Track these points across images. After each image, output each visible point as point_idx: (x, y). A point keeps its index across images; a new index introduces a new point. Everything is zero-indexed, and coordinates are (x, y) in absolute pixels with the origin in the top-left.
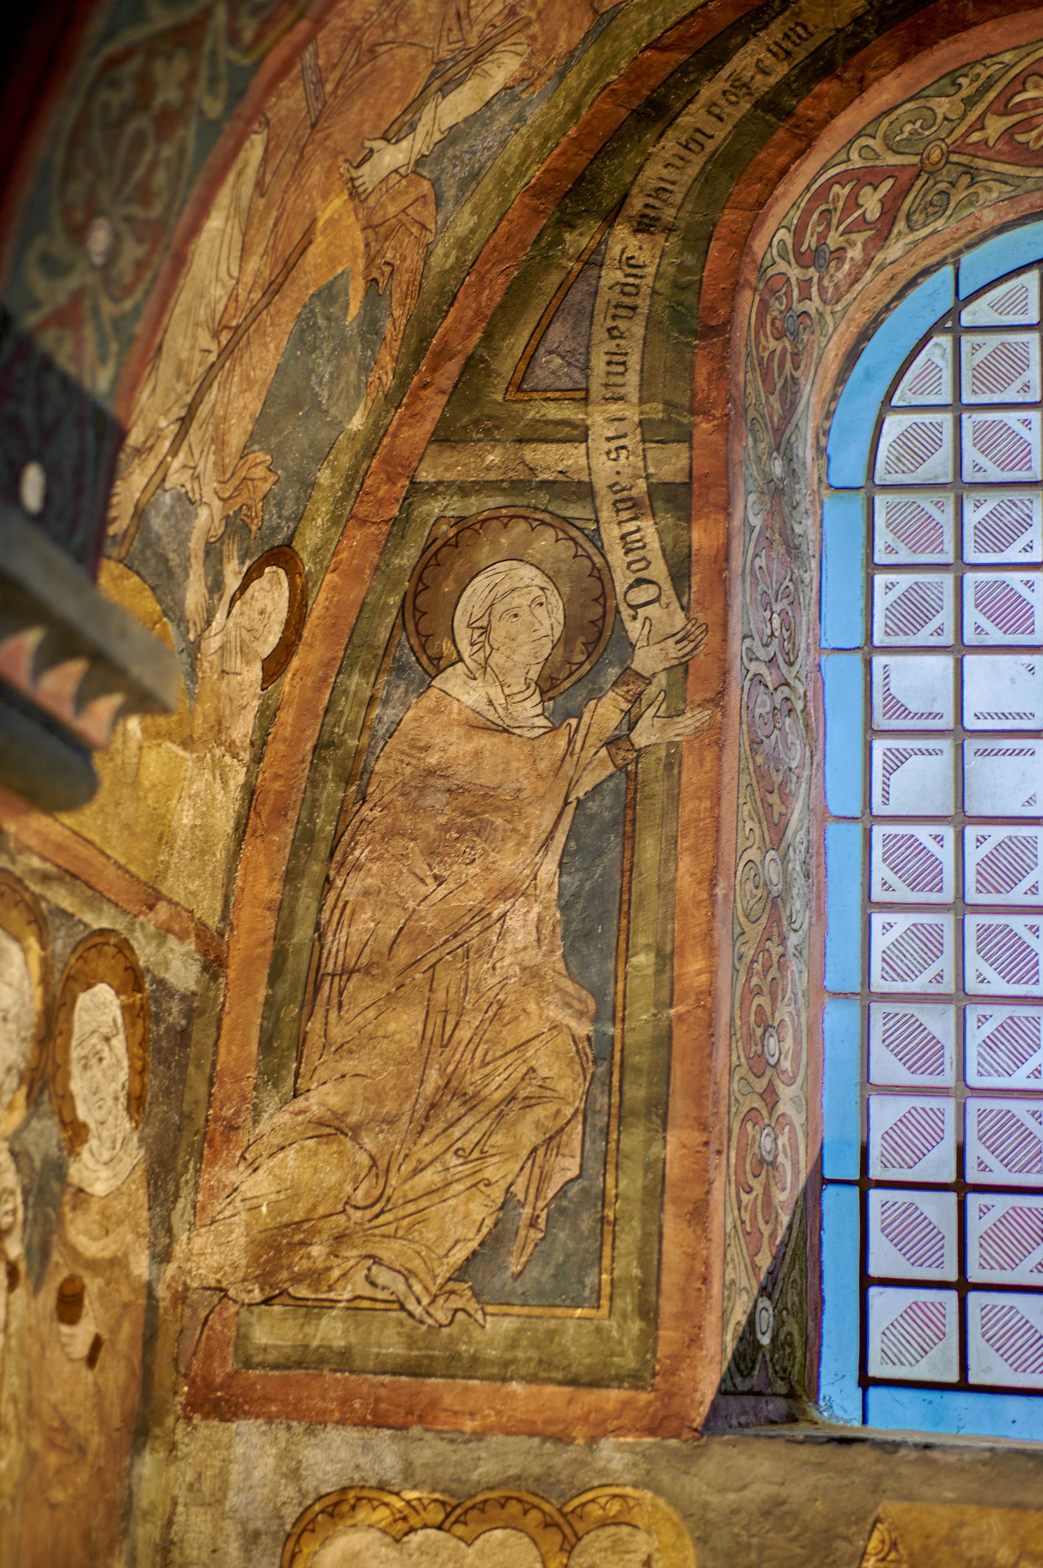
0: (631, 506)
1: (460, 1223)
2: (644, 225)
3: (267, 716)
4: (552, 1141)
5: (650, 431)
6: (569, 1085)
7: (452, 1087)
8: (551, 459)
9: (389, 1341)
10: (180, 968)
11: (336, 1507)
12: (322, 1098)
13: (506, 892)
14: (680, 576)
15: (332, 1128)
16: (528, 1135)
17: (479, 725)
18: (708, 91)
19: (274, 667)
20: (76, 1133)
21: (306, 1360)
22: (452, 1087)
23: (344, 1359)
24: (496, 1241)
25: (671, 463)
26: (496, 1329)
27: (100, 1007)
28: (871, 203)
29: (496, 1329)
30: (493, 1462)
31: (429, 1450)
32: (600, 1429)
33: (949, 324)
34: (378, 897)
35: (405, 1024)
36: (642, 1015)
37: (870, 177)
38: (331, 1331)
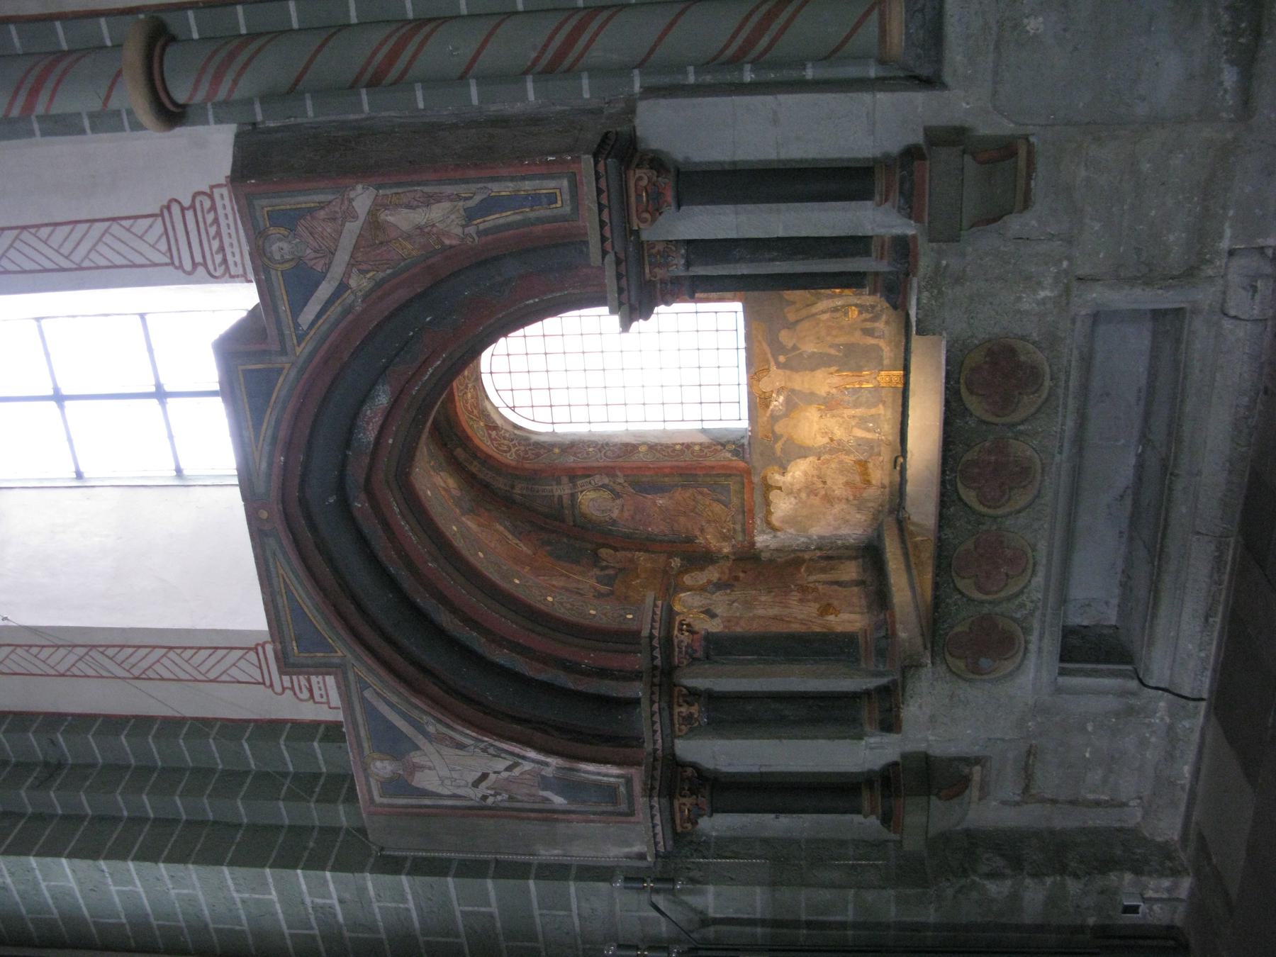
0: (575, 486)
1: (718, 508)
2: (513, 487)
3: (623, 549)
4: (701, 493)
5: (559, 483)
6: (691, 491)
7: (693, 511)
8: (566, 501)
9: (740, 517)
10: (676, 562)
11: (769, 523)
12: (698, 533)
13: (655, 504)
14: (589, 476)
15: (702, 530)
16: (700, 497)
17: (622, 510)
18: (481, 476)
19: (616, 549)
20: (709, 582)
21: (744, 531)
22: (693, 511)
23: (743, 525)
24: (718, 501)
25: (565, 480)
26: (735, 501)
27: (687, 580)
28: (494, 433)
29: (735, 501)
30: (758, 498)
31: (757, 510)
32: (751, 482)
33: (513, 408)
34: (657, 528)
35: (682, 519)
36: (677, 479)
37: (490, 435)
38: (738, 527)
